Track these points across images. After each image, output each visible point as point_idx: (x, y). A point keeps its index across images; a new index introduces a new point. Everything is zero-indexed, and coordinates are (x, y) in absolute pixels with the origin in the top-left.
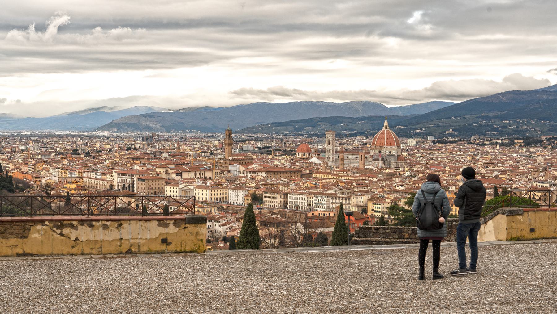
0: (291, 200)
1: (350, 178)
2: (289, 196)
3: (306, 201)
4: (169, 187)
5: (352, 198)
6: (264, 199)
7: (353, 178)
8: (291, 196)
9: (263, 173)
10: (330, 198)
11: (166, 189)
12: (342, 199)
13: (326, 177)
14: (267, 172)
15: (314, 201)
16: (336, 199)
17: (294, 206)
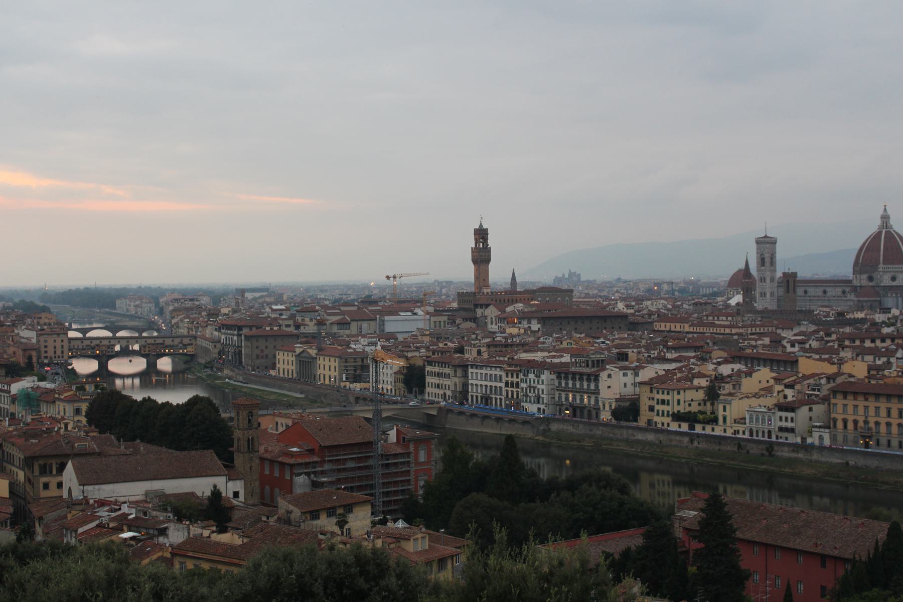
0: (474, 382)
1: (728, 331)
2: (470, 370)
3: (503, 385)
4: (281, 353)
5: (603, 375)
6: (429, 379)
7: (734, 331)
8: (474, 371)
9: (534, 322)
10: (554, 376)
11: (278, 357)
12: (581, 379)
13: (678, 329)
14: (543, 320)
15: (523, 385)
16: (566, 378)
17: (479, 395)
